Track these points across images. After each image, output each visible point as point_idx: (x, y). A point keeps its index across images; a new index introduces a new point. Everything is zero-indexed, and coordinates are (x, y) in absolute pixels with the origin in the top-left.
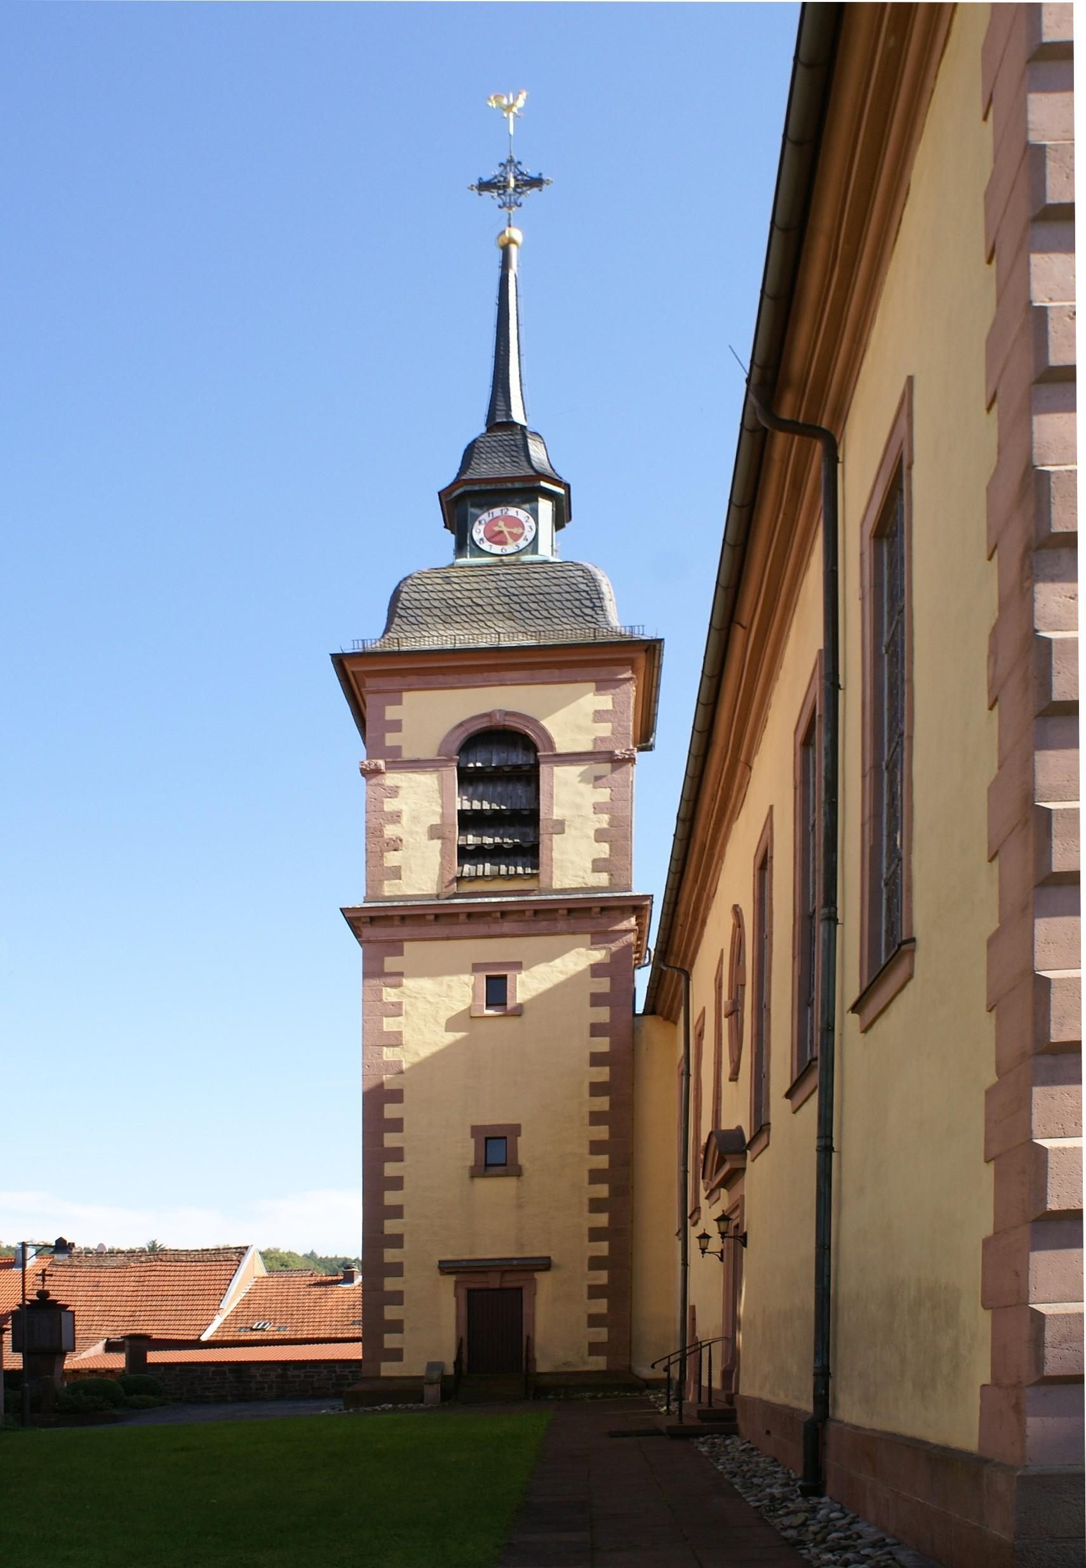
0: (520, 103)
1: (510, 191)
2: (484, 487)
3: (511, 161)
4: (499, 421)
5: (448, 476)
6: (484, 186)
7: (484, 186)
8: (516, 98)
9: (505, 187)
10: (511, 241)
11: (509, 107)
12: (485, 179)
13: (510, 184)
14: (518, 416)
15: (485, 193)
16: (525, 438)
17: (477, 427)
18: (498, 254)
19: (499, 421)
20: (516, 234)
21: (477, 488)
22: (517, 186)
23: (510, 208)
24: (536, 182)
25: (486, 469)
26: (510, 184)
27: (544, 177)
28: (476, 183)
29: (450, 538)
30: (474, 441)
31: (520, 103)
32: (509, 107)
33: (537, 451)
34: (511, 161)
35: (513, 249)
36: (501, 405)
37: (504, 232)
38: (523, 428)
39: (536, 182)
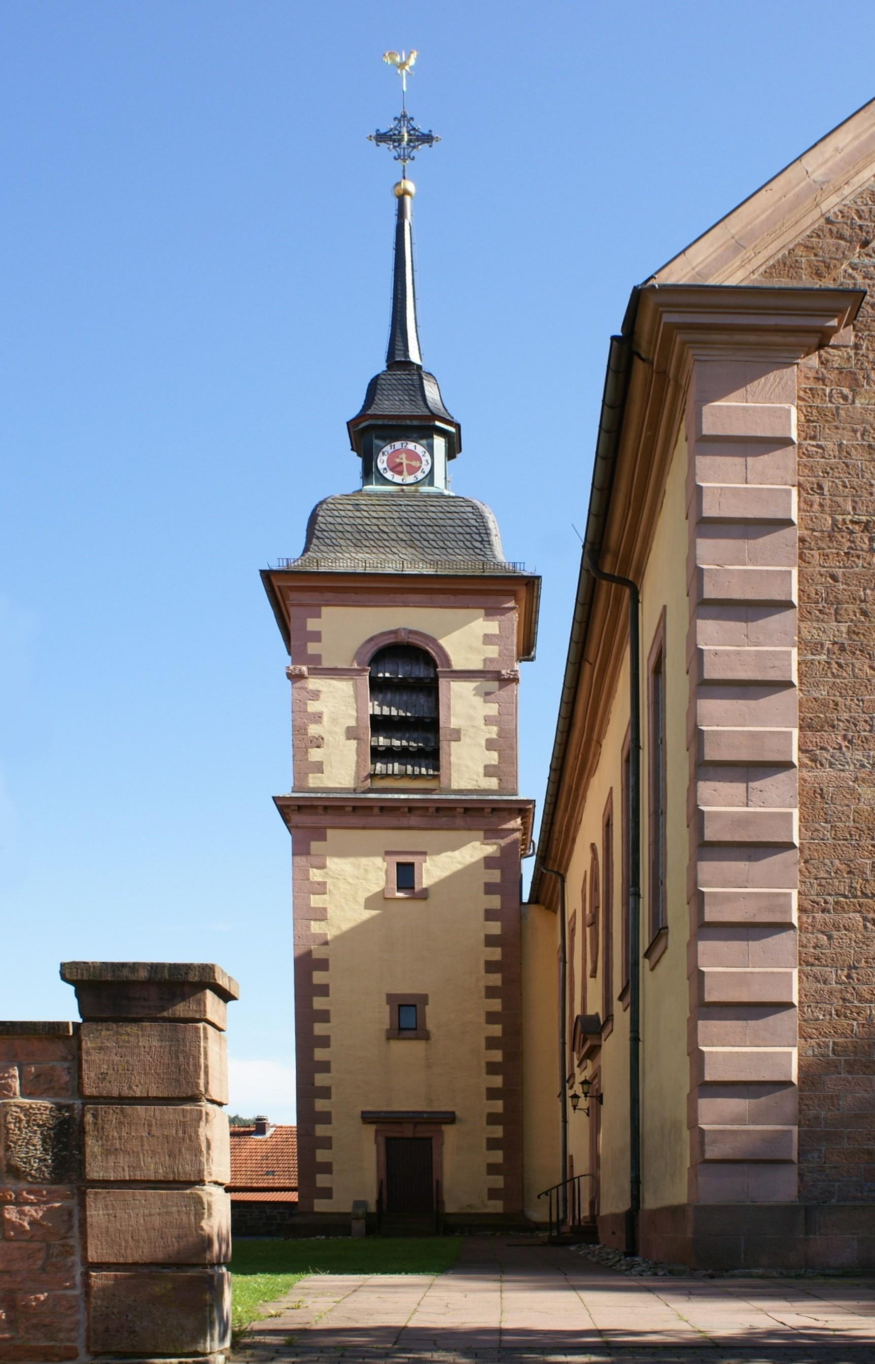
0: (412, 62)
1: (404, 144)
2: (386, 422)
3: (404, 116)
4: (397, 360)
5: (355, 409)
6: (381, 138)
7: (381, 138)
8: (408, 57)
9: (400, 141)
10: (406, 192)
11: (402, 65)
12: (382, 131)
13: (404, 138)
14: (414, 357)
15: (382, 144)
16: (421, 379)
17: (380, 365)
18: (395, 202)
19: (397, 360)
20: (410, 186)
21: (380, 422)
22: (410, 141)
23: (404, 160)
24: (428, 139)
25: (387, 406)
26: (404, 138)
27: (434, 134)
28: (374, 134)
29: (357, 462)
30: (377, 377)
31: (412, 62)
32: (402, 65)
33: (431, 392)
34: (404, 116)
35: (408, 199)
36: (399, 345)
37: (399, 184)
38: (419, 367)
39: (428, 139)
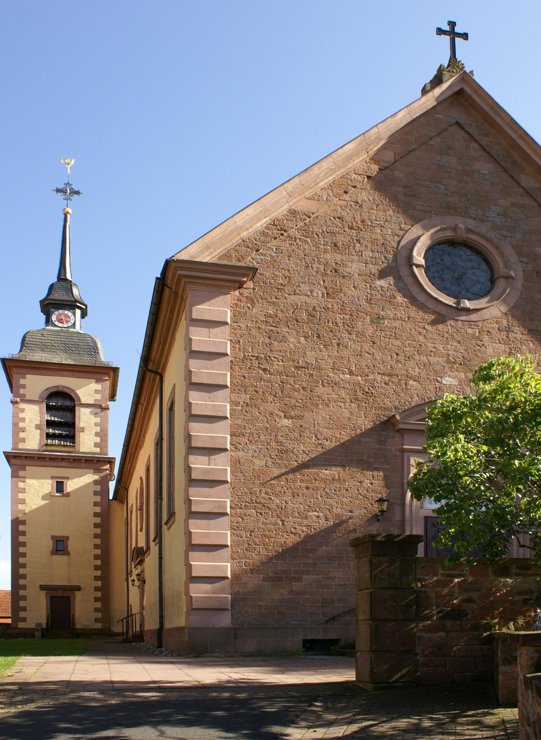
0: (72, 163)
1: (68, 194)
2: (56, 302)
3: (68, 183)
4: (62, 278)
5: (43, 295)
6: (58, 191)
7: (58, 191)
8: (71, 161)
9: (66, 193)
10: (68, 213)
11: (68, 164)
12: (59, 188)
13: (68, 192)
14: (69, 277)
15: (59, 193)
16: (71, 286)
17: (55, 280)
18: (63, 216)
19: (62, 278)
20: (69, 210)
21: (54, 302)
22: (70, 193)
23: (68, 200)
24: (78, 193)
25: (57, 295)
26: (68, 192)
27: (80, 192)
28: (55, 189)
29: (43, 317)
30: (53, 284)
31: (72, 163)
32: (68, 164)
33: (75, 291)
34: (68, 183)
35: (68, 215)
36: (63, 272)
37: (65, 209)
38: (71, 281)
39: (78, 193)
